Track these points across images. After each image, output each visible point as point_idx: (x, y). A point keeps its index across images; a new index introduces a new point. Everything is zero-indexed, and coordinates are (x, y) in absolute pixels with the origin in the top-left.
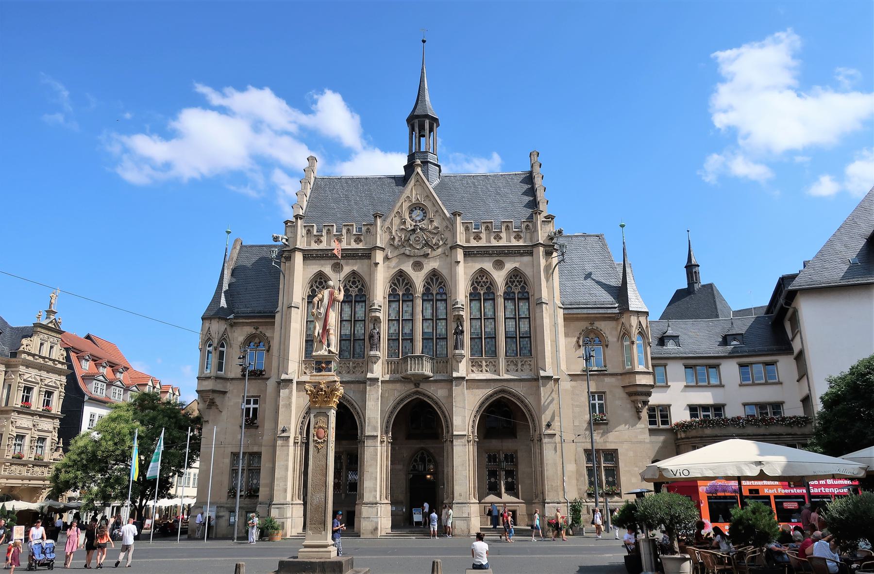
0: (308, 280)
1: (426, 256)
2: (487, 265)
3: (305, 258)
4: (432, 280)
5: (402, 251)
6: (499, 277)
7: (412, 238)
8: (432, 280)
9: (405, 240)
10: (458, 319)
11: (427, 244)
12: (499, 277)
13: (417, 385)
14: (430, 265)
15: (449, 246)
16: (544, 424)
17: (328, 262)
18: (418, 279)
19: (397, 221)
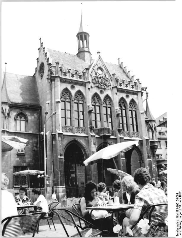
1: (105, 89)
2: (124, 95)
5: (97, 85)
6: (128, 100)
12: (128, 100)
13: (105, 140)
14: (106, 93)
15: (111, 87)
18: (102, 97)
19: (94, 72)
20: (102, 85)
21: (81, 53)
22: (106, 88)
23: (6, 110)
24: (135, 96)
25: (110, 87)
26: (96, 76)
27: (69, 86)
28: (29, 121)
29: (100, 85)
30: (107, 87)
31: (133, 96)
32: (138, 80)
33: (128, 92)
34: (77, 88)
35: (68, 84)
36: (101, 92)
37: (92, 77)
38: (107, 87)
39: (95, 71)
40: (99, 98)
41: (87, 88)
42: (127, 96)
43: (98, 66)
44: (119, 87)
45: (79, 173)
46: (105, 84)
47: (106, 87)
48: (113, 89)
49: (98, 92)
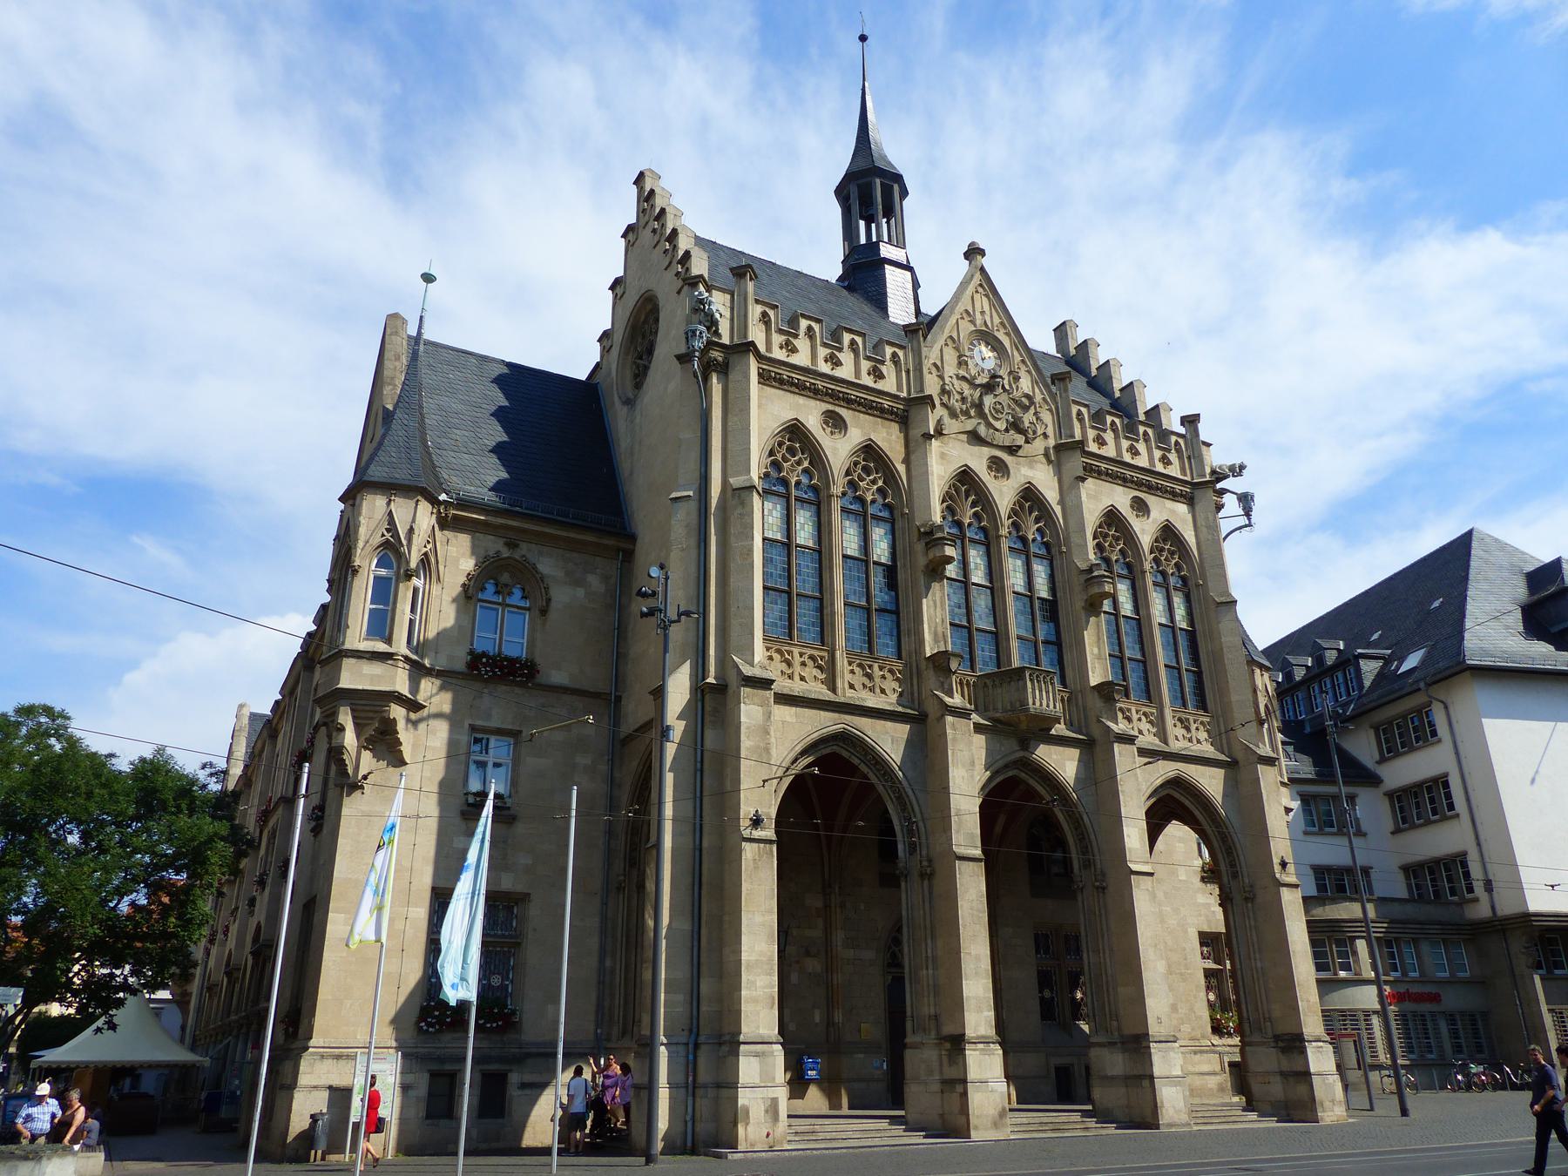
0: (769, 433)
1: (1013, 450)
3: (764, 378)
4: (1022, 506)
7: (988, 401)
8: (1022, 506)
9: (974, 405)
10: (1091, 605)
11: (1016, 426)
15: (1051, 442)
16: (1276, 861)
17: (812, 403)
18: (1004, 494)
19: (950, 356)
20: (998, 425)
21: (864, 272)
22: (1020, 447)
23: (411, 531)
24: (1182, 508)
25: (1039, 445)
26: (962, 373)
27: (811, 414)
28: (553, 615)
29: (989, 425)
30: (1027, 442)
31: (1169, 504)
32: (1191, 421)
33: (1147, 484)
34: (861, 429)
35: (801, 400)
36: (998, 467)
37: (941, 377)
38: (1027, 442)
39: (957, 349)
40: (983, 500)
41: (916, 433)
42: (1140, 507)
43: (973, 322)
44: (1093, 447)
45: (849, 954)
46: (1016, 426)
47: (1020, 440)
48: (1058, 458)
49: (978, 460)
